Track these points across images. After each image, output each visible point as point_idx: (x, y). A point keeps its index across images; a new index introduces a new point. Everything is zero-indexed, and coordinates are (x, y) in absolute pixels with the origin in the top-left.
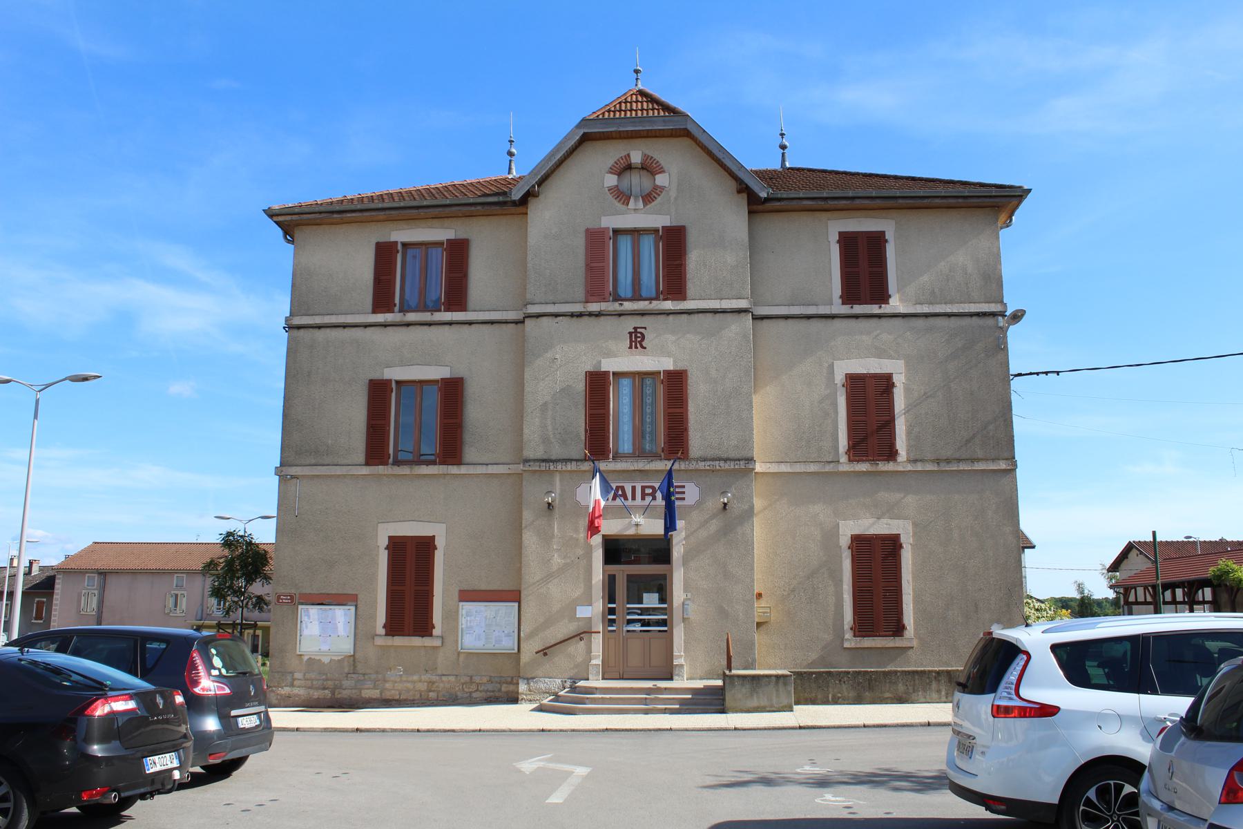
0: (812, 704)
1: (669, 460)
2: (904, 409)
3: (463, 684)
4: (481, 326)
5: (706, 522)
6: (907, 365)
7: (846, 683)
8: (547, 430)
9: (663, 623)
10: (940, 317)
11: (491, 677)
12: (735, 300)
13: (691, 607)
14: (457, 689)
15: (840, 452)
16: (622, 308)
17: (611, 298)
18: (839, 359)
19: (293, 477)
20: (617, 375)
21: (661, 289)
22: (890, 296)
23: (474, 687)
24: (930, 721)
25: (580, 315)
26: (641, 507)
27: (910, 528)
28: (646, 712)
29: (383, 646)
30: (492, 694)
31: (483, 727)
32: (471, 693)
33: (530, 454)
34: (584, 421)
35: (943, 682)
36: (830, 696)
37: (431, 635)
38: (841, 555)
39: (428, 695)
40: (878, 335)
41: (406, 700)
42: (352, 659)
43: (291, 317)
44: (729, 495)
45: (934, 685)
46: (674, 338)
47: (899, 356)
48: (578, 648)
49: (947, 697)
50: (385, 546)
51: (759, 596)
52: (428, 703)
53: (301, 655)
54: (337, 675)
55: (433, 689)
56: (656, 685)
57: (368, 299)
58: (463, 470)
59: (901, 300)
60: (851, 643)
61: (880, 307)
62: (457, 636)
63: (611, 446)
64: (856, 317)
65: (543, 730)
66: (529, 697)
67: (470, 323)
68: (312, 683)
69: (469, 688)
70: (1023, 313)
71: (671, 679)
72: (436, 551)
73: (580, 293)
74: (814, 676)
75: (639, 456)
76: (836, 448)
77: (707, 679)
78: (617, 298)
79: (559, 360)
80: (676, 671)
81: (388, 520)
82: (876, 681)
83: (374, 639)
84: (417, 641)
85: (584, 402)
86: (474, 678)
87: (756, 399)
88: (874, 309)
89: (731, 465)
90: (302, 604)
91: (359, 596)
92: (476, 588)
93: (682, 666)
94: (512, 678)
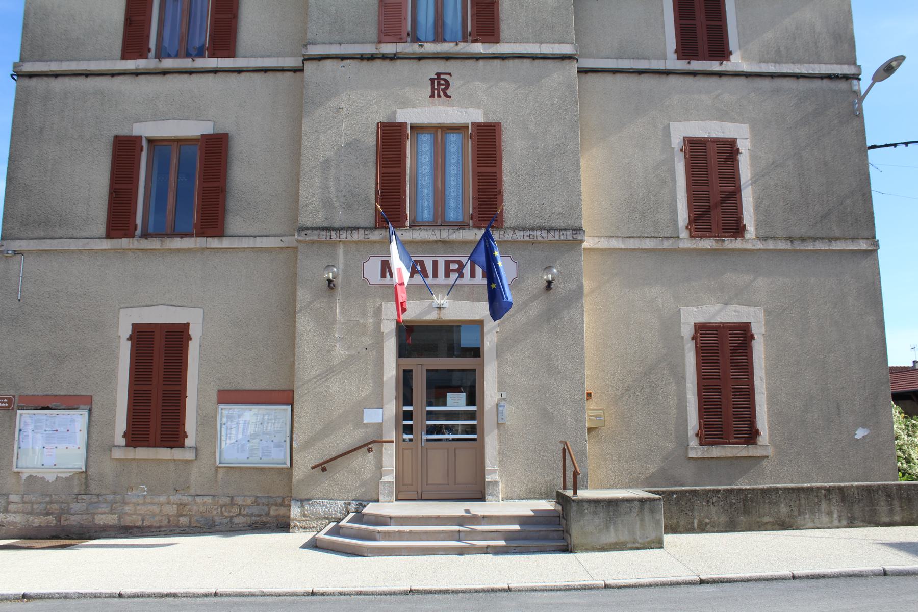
0: (672, 533)
1: (480, 228)
2: (751, 179)
3: (222, 507)
4: (252, 74)
5: (526, 304)
6: (752, 129)
7: (716, 504)
8: (329, 192)
9: (472, 429)
10: (788, 79)
11: (258, 497)
12: (557, 45)
13: (508, 411)
14: (214, 512)
15: (680, 226)
16: (422, 50)
17: (409, 39)
18: (676, 120)
19: (16, 253)
20: (417, 129)
21: (469, 30)
22: (731, 53)
23: (235, 510)
24: (887, 568)
25: (372, 58)
26: (444, 286)
27: (761, 315)
28: (461, 552)
29: (123, 459)
30: (258, 518)
31: (221, 590)
32: (232, 517)
33: (306, 220)
34: (374, 182)
35: (834, 501)
36: (696, 521)
37: (182, 446)
38: (684, 348)
39: (179, 521)
40: (718, 95)
41: (149, 527)
42: (84, 476)
43: (21, 63)
44: (555, 271)
45: (824, 506)
46: (485, 86)
47: (743, 119)
48: (364, 462)
49: (840, 521)
50: (128, 336)
51: (589, 395)
52: (178, 530)
53: (19, 472)
54: (64, 497)
55: (184, 513)
56: (467, 511)
57: (117, 42)
58: (226, 243)
59: (743, 58)
60: (697, 452)
61: (721, 64)
62: (215, 446)
63: (408, 212)
64: (694, 74)
65: (313, 593)
66: (304, 524)
67: (239, 71)
68: (32, 507)
69: (230, 512)
70: (900, 59)
71: (482, 499)
72: (190, 342)
73: (372, 31)
74: (675, 496)
75: (442, 226)
76: (675, 222)
77: (528, 499)
78: (416, 40)
79: (345, 110)
80: (488, 490)
81: (132, 305)
82: (752, 501)
83: (111, 451)
84: (164, 453)
85: (375, 158)
86: (235, 498)
87: (583, 163)
88: (715, 66)
89: (557, 236)
90: (22, 408)
91: (94, 398)
92: (239, 388)
93: (496, 483)
94: (283, 498)
